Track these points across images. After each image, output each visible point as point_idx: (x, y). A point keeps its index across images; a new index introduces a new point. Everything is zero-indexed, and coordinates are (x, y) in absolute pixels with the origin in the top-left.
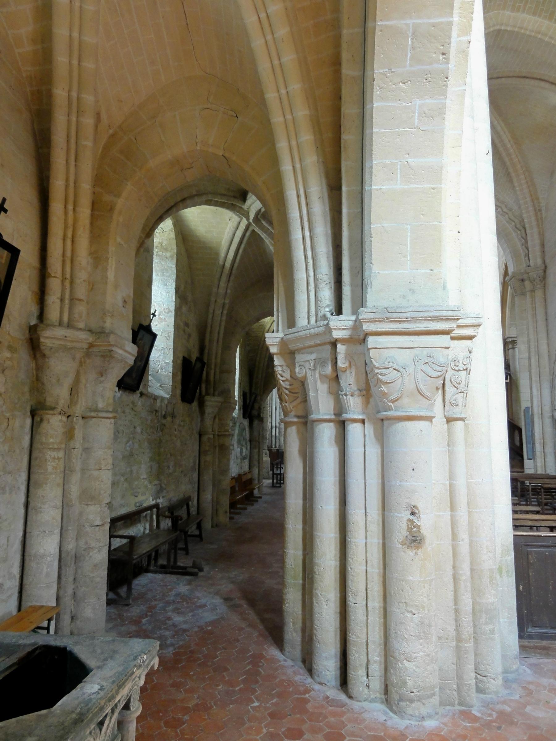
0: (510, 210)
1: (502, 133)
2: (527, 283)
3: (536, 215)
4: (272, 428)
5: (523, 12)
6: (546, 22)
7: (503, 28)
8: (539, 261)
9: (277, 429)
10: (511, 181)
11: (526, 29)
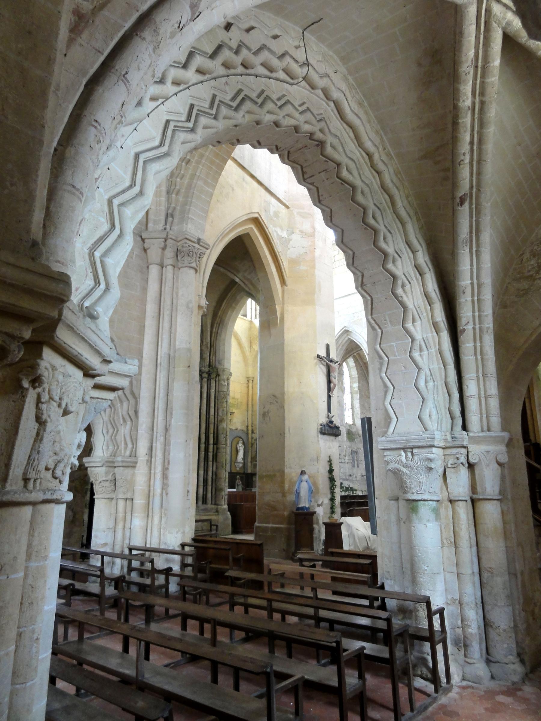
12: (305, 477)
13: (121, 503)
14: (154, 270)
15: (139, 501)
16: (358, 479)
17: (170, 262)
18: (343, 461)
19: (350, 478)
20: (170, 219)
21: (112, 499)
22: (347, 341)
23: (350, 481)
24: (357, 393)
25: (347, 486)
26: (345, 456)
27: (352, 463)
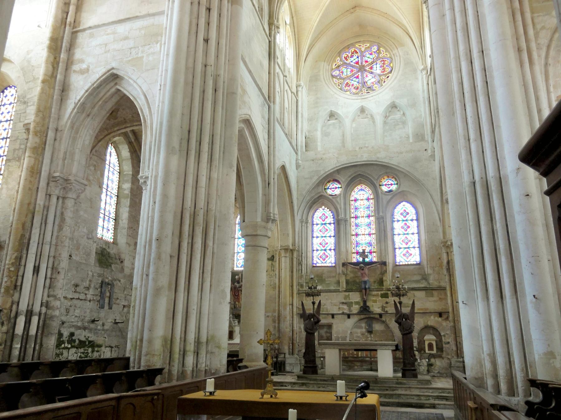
4: (16, 317)
9: (35, 320)
16: (106, 327)
18: (82, 296)
19: (92, 326)
22: (113, 95)
23: (91, 330)
24: (127, 198)
25: (83, 339)
26: (88, 288)
27: (99, 301)
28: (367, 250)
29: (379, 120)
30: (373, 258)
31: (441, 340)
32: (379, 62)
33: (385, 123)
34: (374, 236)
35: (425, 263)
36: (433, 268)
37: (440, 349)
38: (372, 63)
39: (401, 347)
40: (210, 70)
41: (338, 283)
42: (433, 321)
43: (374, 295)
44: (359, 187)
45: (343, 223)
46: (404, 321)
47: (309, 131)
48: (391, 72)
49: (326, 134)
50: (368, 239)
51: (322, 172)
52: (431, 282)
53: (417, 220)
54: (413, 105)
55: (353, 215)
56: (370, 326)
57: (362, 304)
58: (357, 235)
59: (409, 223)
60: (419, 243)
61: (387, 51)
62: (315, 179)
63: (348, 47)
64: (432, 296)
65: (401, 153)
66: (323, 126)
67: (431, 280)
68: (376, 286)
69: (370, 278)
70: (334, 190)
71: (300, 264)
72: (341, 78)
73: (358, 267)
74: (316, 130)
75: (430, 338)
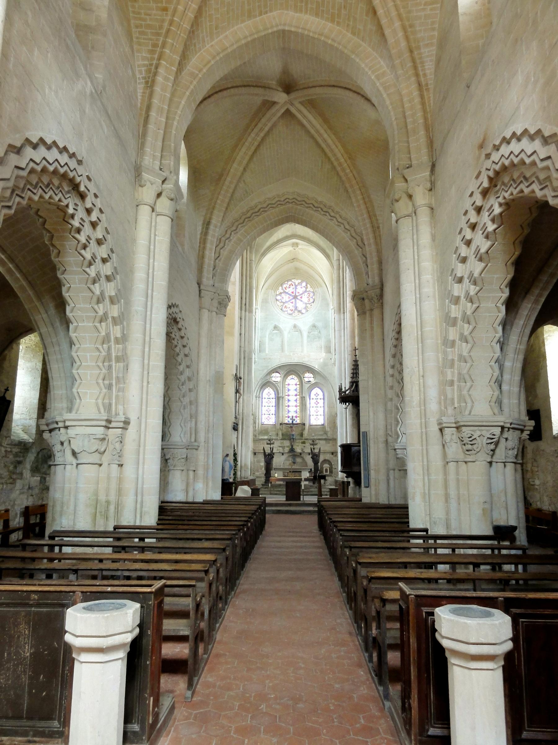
0: (352, 227)
1: (333, 147)
2: (367, 301)
3: (374, 232)
5: (306, 12)
6: (330, 24)
7: (287, 28)
8: (377, 280)
10: (350, 198)
11: (309, 31)
12: (228, 459)
13: (191, 473)
14: (205, 314)
15: (200, 472)
17: (215, 309)
20: (214, 278)
21: (183, 470)
28: (295, 415)
29: (305, 334)
30: (298, 421)
31: (332, 468)
32: (306, 294)
33: (308, 337)
34: (298, 407)
35: (326, 424)
36: (330, 428)
37: (331, 472)
38: (302, 294)
39: (313, 469)
40: (242, 350)
41: (278, 434)
42: (328, 457)
43: (298, 442)
44: (291, 376)
45: (281, 399)
46: (315, 457)
47: (261, 337)
48: (313, 302)
49: (271, 340)
50: (295, 409)
51: (270, 367)
52: (329, 435)
53: (324, 399)
54: (326, 327)
55: (287, 394)
56: (294, 459)
57: (290, 447)
58: (289, 406)
59: (319, 401)
60: (324, 413)
61: (311, 287)
62: (265, 372)
63: (288, 281)
64: (329, 443)
65: (317, 359)
66: (270, 334)
67: (329, 434)
68: (298, 437)
69: (296, 432)
70: (276, 377)
71: (255, 423)
72: (282, 302)
73: (289, 426)
74: (266, 337)
75: (326, 466)
